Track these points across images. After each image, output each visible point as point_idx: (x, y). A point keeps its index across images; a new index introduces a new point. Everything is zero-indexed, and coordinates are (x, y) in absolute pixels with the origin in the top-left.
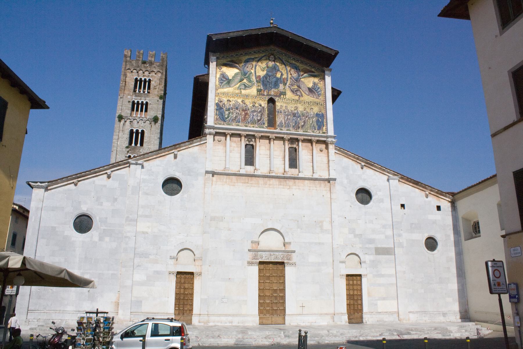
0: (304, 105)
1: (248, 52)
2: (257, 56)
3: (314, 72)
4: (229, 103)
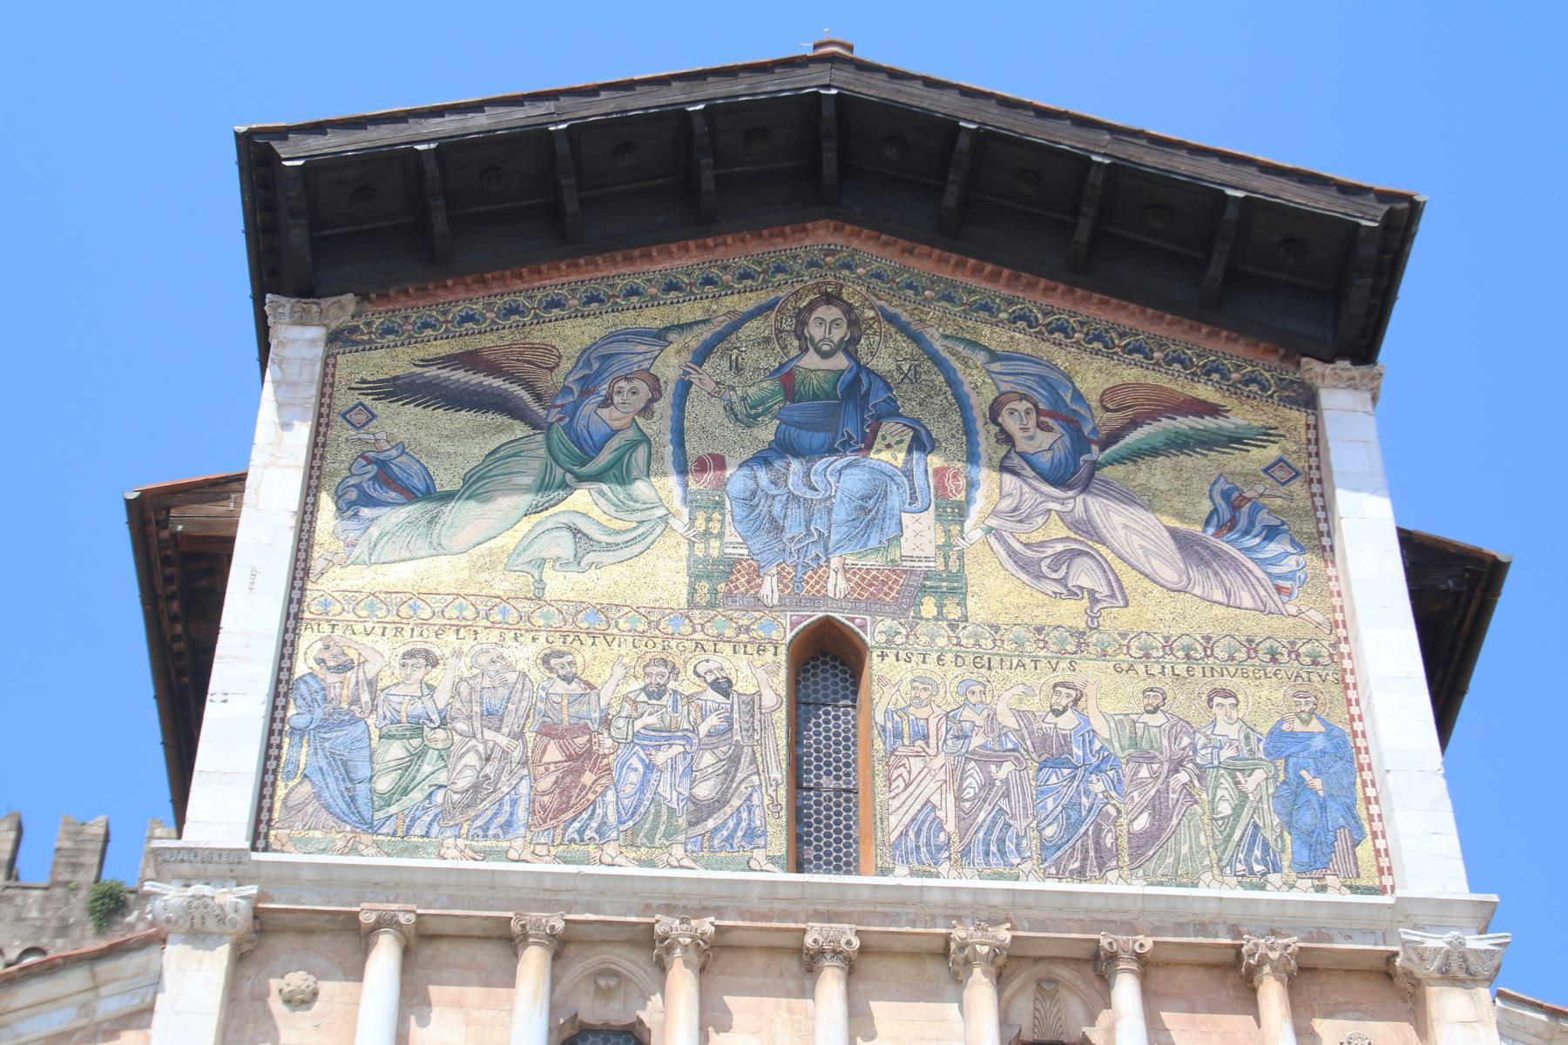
0: (1141, 668)
2: (690, 311)
3: (1214, 410)
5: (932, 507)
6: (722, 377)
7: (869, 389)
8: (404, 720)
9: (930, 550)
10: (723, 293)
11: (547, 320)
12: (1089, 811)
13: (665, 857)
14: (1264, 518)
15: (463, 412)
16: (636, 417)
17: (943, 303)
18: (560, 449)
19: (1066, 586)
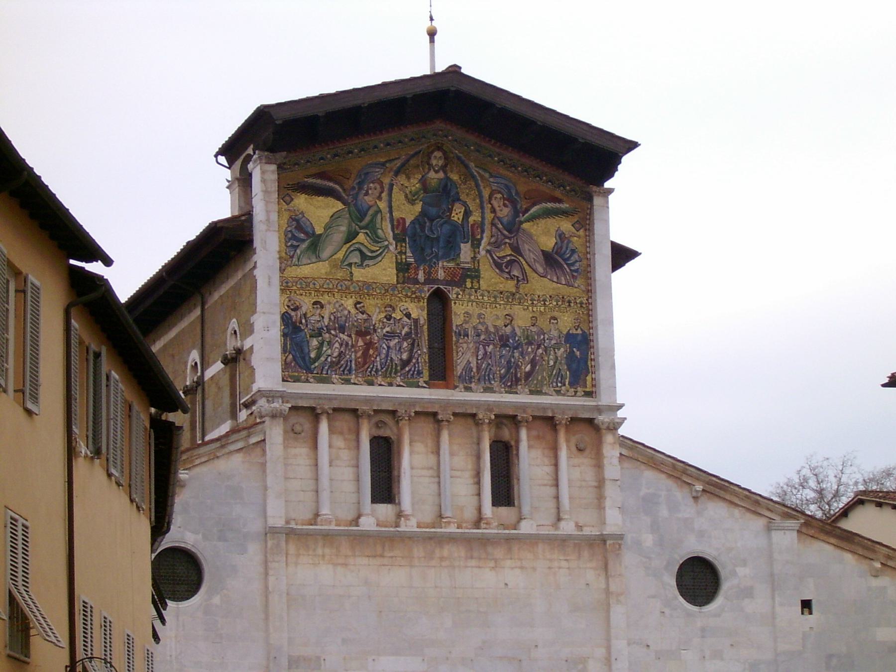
0: (530, 308)
1: (369, 144)
3: (560, 201)
4: (318, 311)
5: (470, 242)
9: (469, 260)
13: (395, 381)
15: (320, 197)
19: (510, 275)
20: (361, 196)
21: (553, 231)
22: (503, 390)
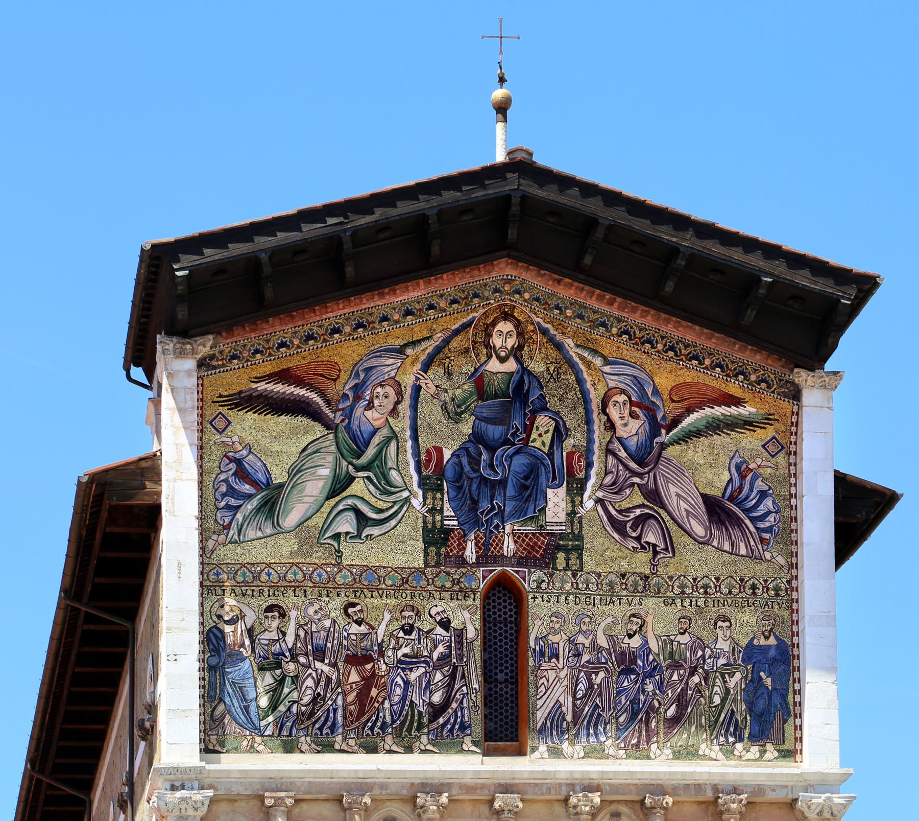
3: (737, 402)
6: (440, 382)
7: (529, 388)
8: (271, 657)
9: (562, 517)
10: (440, 315)
11: (331, 343)
12: (644, 704)
13: (417, 744)
14: (760, 485)
15: (283, 417)
16: (388, 417)
17: (578, 320)
18: (344, 446)
20: (359, 411)
21: (724, 459)
22: (622, 752)
